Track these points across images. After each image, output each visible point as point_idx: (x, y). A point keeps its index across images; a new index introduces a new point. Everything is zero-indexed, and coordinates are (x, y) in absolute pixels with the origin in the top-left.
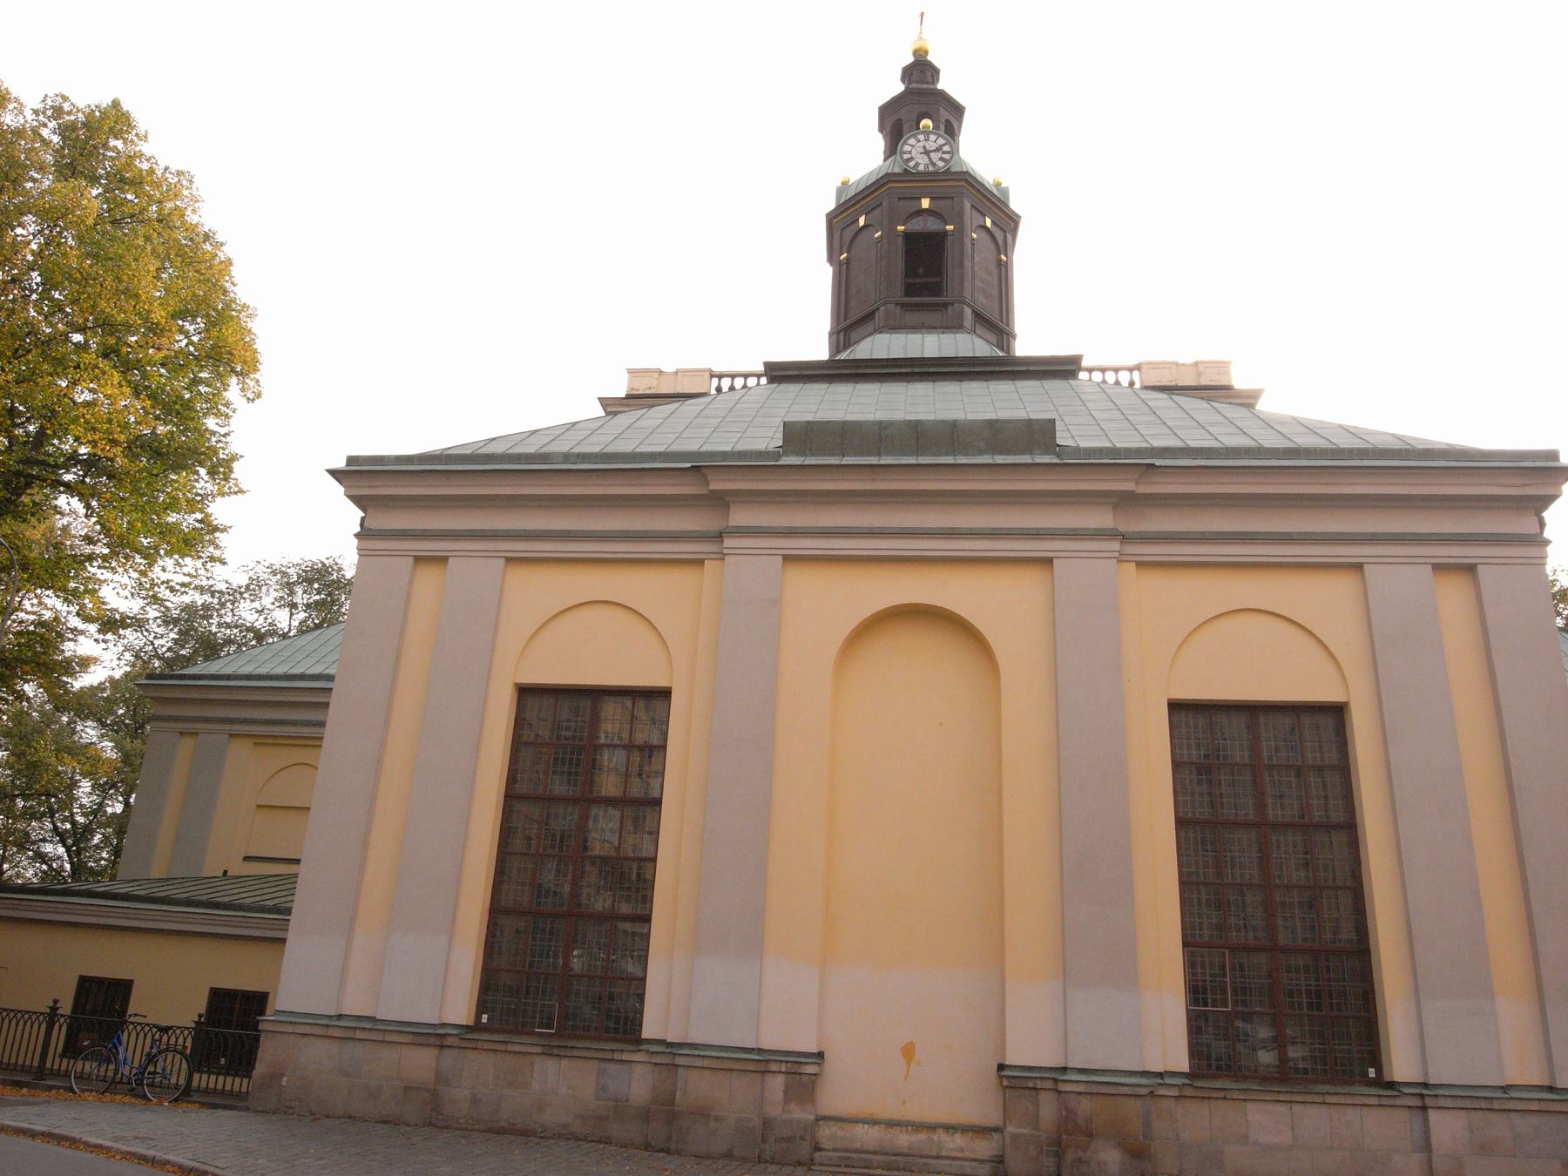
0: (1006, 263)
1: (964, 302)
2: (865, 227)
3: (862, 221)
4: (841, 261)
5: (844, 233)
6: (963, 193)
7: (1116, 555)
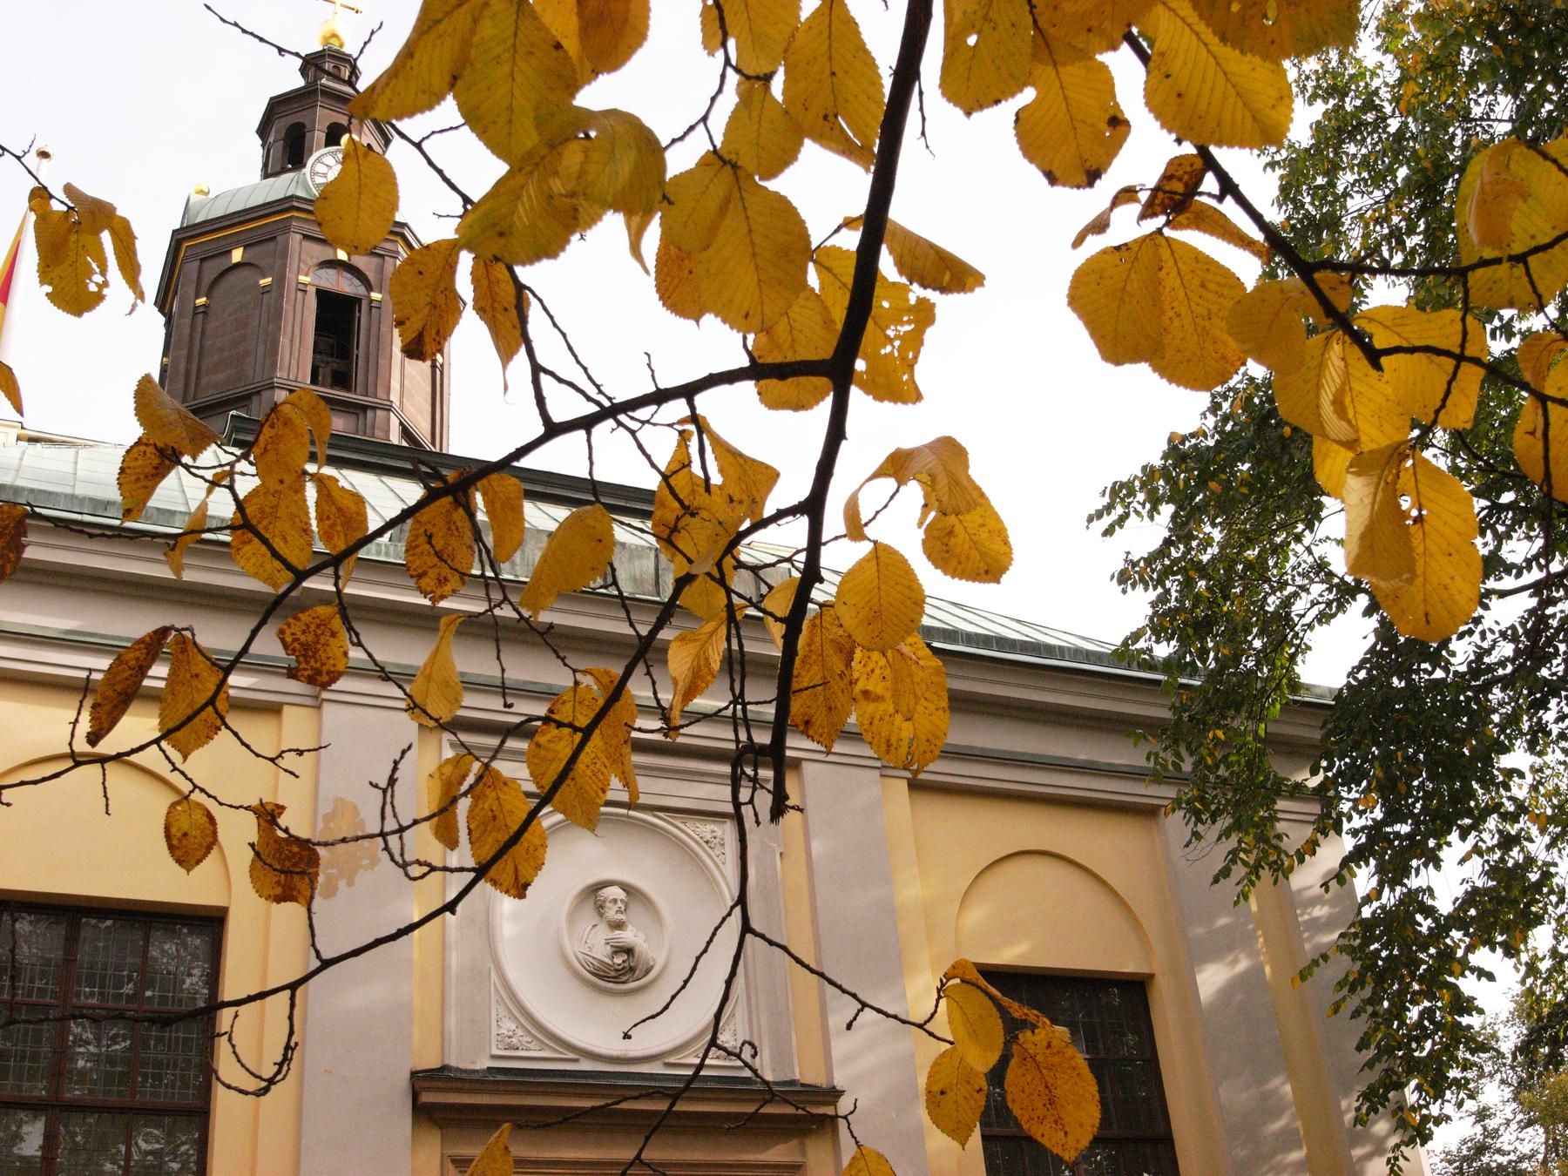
0: (442, 366)
1: (388, 409)
2: (238, 265)
3: (237, 255)
4: (196, 308)
5: (208, 265)
6: (398, 253)
7: (878, 764)
